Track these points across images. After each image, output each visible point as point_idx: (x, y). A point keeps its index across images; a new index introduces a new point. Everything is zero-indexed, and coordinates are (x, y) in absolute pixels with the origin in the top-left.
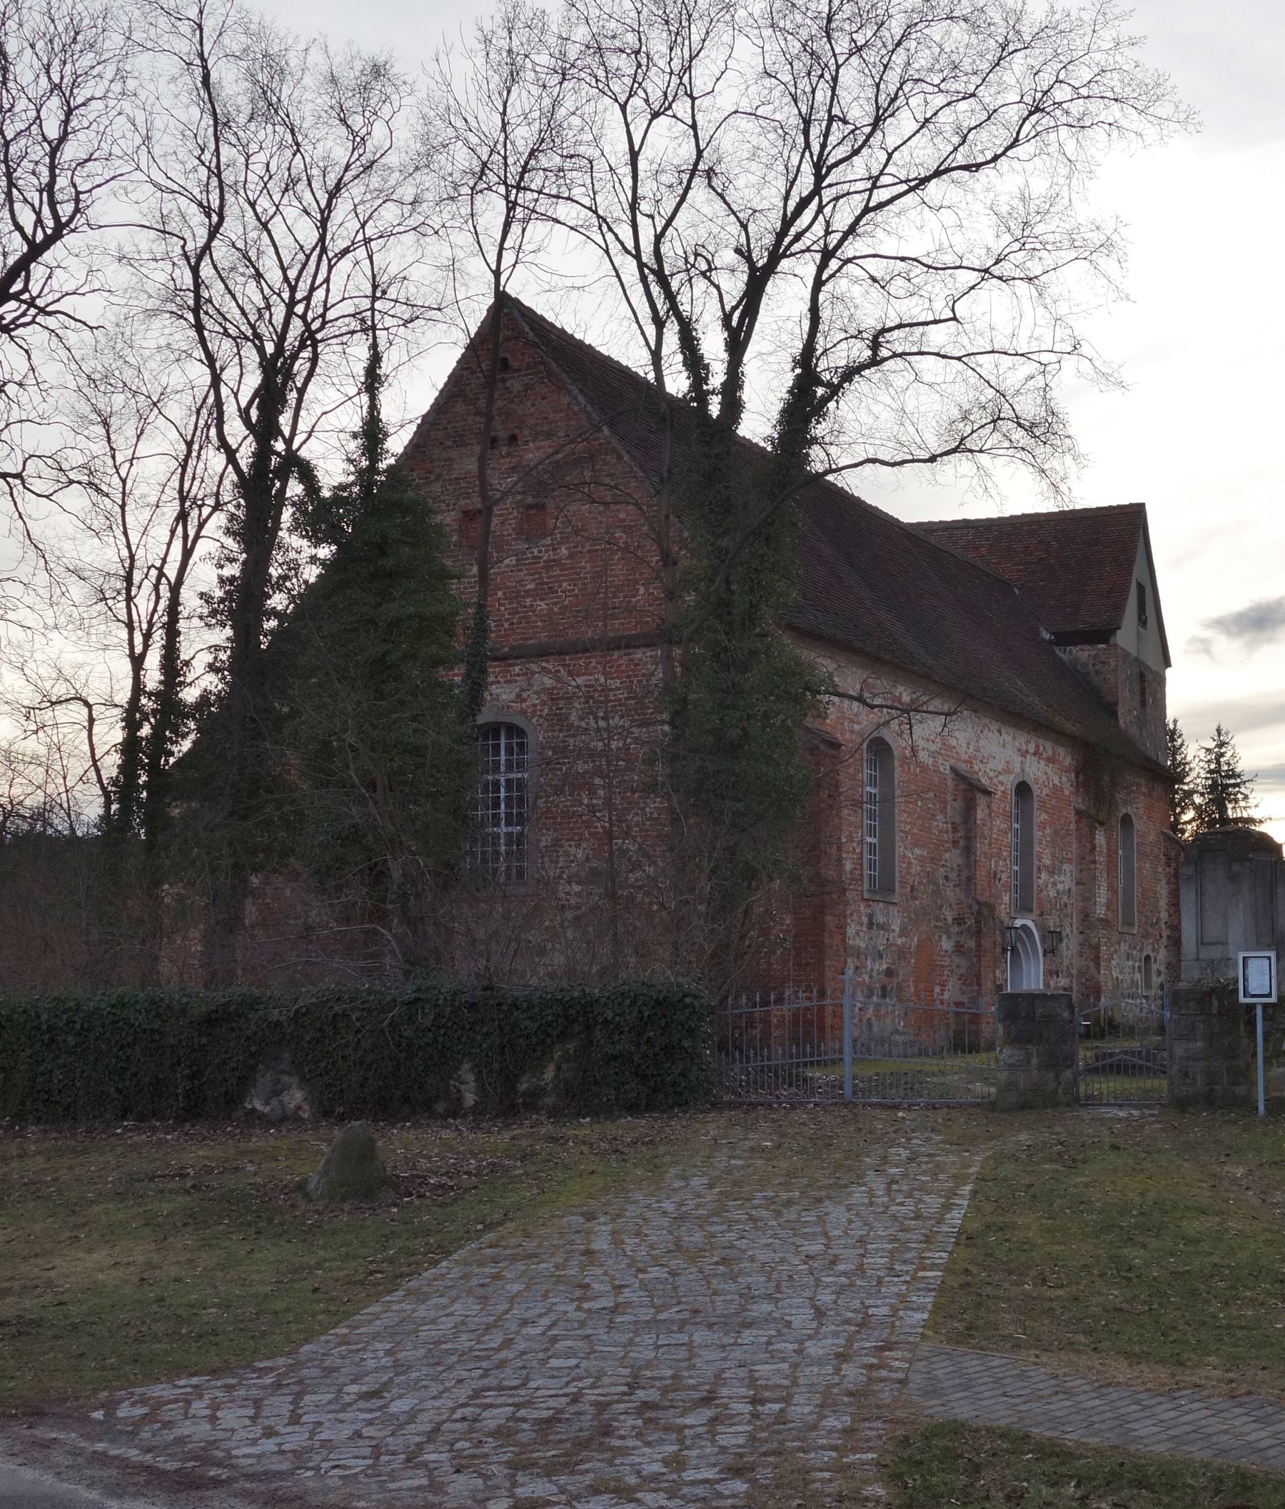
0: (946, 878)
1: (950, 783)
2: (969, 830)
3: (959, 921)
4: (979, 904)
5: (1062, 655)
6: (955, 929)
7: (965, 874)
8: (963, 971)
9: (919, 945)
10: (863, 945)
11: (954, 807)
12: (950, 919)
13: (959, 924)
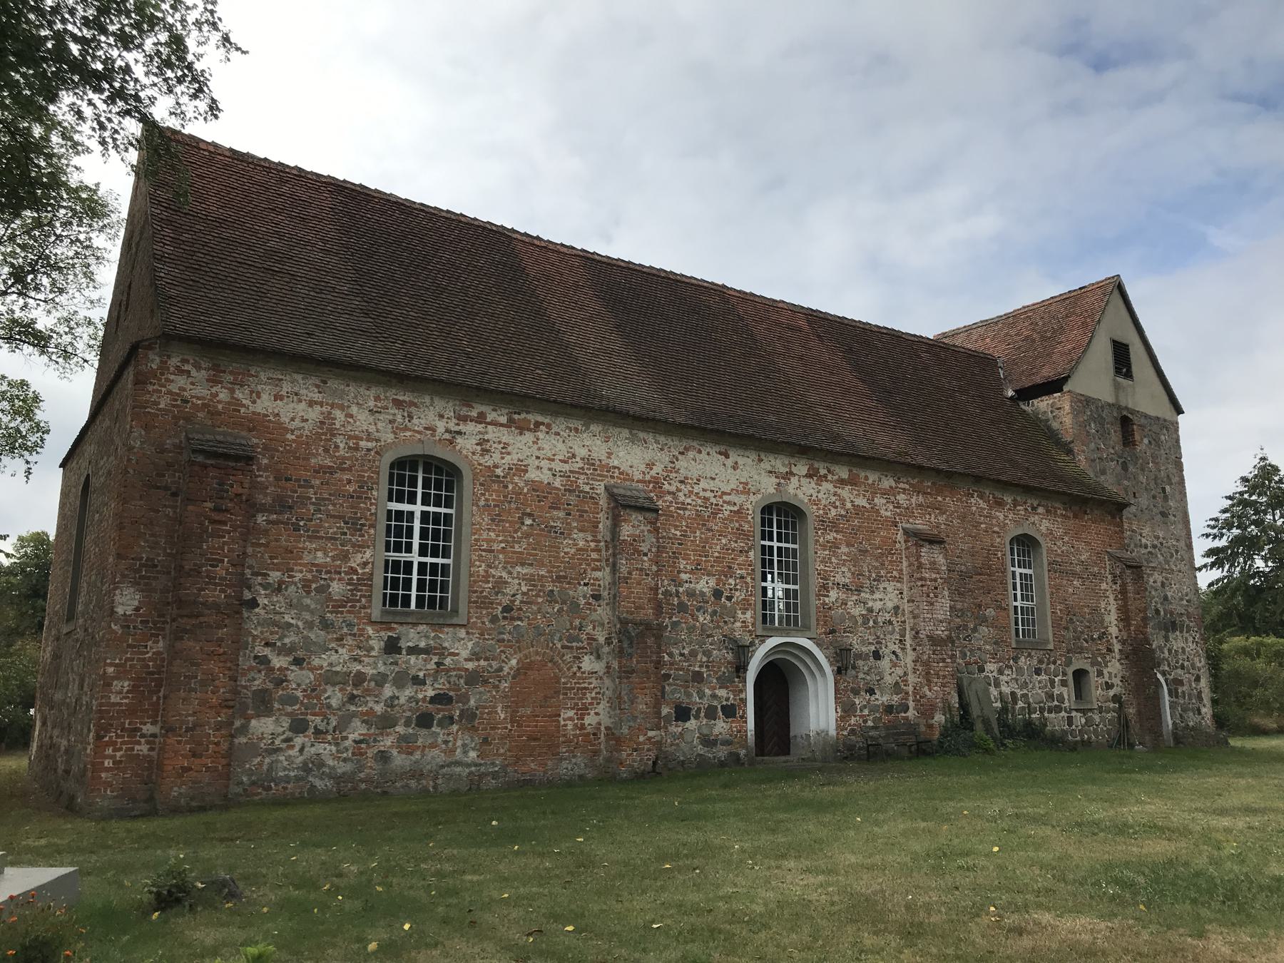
0: (597, 597)
1: (603, 502)
3: (608, 641)
5: (1026, 408)
6: (606, 649)
10: (369, 671)
12: (602, 640)
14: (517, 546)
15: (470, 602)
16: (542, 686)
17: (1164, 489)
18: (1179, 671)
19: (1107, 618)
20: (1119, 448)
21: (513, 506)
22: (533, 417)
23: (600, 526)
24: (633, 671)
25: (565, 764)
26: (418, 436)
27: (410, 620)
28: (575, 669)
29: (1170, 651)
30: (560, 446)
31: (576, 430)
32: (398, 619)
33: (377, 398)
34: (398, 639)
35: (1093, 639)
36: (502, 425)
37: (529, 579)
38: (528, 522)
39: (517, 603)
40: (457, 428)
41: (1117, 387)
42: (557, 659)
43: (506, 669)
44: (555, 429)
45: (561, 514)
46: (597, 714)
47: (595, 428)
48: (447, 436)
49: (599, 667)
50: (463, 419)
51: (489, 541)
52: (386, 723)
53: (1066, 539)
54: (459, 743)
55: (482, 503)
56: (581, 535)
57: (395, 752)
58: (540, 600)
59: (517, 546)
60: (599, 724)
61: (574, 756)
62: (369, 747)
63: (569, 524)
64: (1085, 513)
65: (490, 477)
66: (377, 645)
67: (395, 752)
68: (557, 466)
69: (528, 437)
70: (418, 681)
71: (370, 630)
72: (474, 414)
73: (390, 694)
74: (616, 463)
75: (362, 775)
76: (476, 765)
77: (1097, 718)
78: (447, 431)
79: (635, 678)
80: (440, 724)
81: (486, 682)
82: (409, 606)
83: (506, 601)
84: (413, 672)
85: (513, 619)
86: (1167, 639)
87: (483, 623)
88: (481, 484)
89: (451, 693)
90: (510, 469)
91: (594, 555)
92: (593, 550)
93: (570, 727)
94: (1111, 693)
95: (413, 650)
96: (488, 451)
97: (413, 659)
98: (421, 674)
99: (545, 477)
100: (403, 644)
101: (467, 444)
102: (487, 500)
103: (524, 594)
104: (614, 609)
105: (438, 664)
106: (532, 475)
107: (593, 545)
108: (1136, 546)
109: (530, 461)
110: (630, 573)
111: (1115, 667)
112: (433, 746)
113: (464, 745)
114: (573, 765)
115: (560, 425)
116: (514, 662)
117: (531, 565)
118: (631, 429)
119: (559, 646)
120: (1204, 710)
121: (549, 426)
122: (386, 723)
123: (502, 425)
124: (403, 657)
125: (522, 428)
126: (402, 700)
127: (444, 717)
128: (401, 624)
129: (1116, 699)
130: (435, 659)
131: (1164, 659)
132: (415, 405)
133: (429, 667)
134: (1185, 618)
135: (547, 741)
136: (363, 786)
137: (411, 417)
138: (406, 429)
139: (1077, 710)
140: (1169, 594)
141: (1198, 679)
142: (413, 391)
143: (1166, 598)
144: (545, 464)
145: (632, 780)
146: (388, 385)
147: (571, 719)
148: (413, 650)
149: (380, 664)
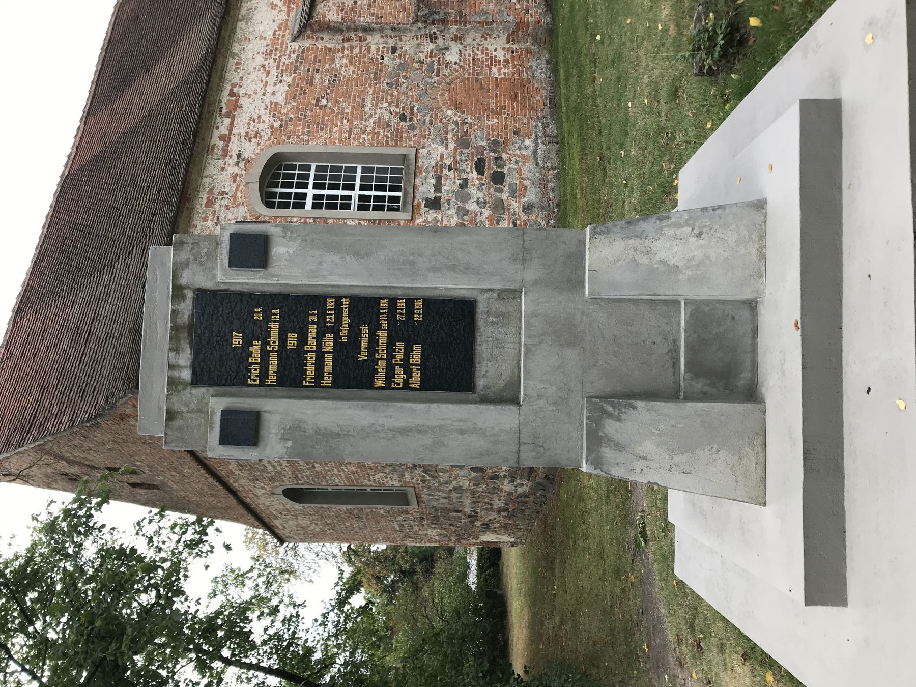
0: (394, 50)
1: (307, 43)
2: (348, 29)
3: (433, 38)
4: (416, 21)
6: (440, 41)
7: (389, 32)
8: (478, 36)
9: (457, 106)
11: (329, 41)
12: (432, 46)
13: (436, 38)
14: (346, 111)
15: (396, 146)
16: (470, 91)
21: (309, 113)
22: (225, 97)
23: (329, 46)
24: (460, 13)
25: (537, 74)
26: (242, 187)
27: (411, 191)
28: (457, 66)
30: (252, 77)
31: (237, 63)
32: (410, 199)
33: (205, 219)
34: (427, 199)
36: (232, 122)
37: (377, 100)
38: (324, 102)
39: (398, 110)
40: (235, 157)
42: (448, 80)
43: (455, 118)
44: (237, 81)
45: (317, 76)
46: (496, 50)
47: (236, 48)
48: (242, 165)
49: (455, 48)
50: (226, 152)
51: (341, 132)
52: (499, 207)
54: (518, 152)
55: (306, 137)
56: (337, 61)
57: (524, 200)
58: (395, 93)
59: (346, 111)
60: (504, 49)
61: (531, 67)
62: (520, 219)
63: (327, 71)
65: (282, 130)
66: (432, 215)
67: (524, 200)
68: (272, 78)
69: (243, 101)
70: (464, 184)
71: (419, 221)
72: (221, 144)
73: (475, 204)
74: (271, 33)
75: (543, 223)
76: (537, 140)
78: (237, 164)
79: (466, 11)
80: (502, 167)
81: (466, 133)
82: (399, 197)
83: (395, 119)
84: (456, 188)
85: (412, 114)
87: (415, 136)
88: (288, 138)
89: (476, 159)
90: (274, 116)
91: (356, 51)
92: (352, 52)
93: (506, 71)
95: (438, 188)
96: (257, 133)
97: (444, 188)
98: (458, 182)
99: (282, 89)
100: (432, 195)
101: (249, 149)
102: (303, 134)
103: (390, 105)
104: (405, 30)
105: (450, 169)
106: (280, 98)
107: (346, 52)
109: (267, 101)
110: (372, 15)
112: (519, 171)
113: (520, 148)
114: (538, 68)
115: (232, 76)
116: (450, 113)
117: (363, 100)
118: (238, 20)
119: (436, 79)
121: (234, 85)
122: (499, 207)
123: (232, 122)
124: (444, 196)
125: (236, 106)
126: (481, 195)
127: (496, 164)
128: (414, 197)
130: (445, 171)
132: (211, 190)
133: (452, 176)
135: (518, 90)
136: (552, 222)
137: (223, 193)
138: (234, 197)
142: (199, 192)
144: (270, 89)
145: (552, 13)
146: (191, 210)
147: (500, 69)
148: (438, 188)
149: (449, 212)
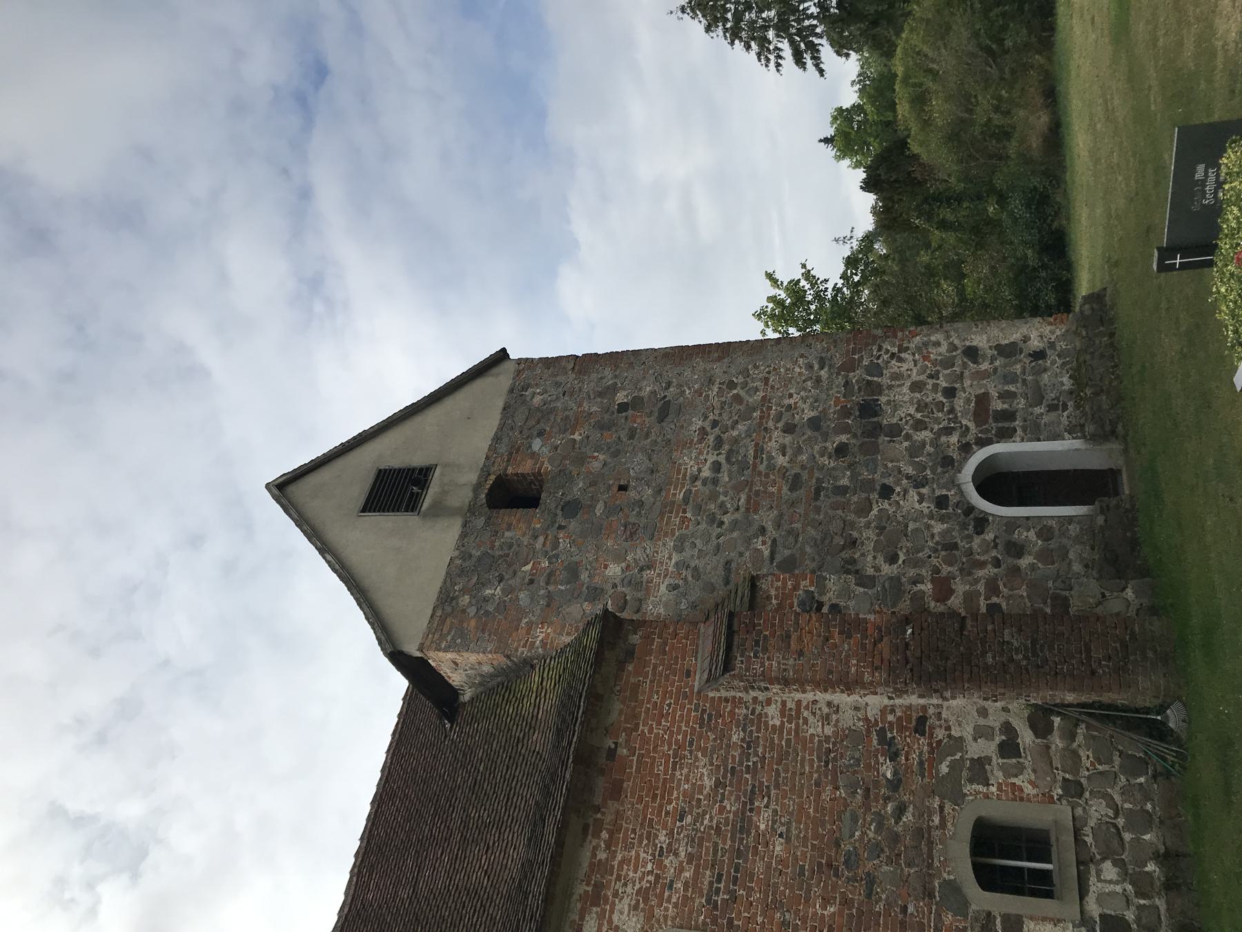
17: (623, 407)
18: (959, 403)
19: (848, 719)
20: (537, 519)
29: (919, 425)
35: (895, 785)
41: (439, 510)
53: (662, 838)
64: (612, 753)
77: (1097, 810)
86: (894, 431)
94: (1026, 737)
108: (713, 496)
111: (963, 713)
120: (1035, 344)
129: (1040, 721)
131: (935, 443)
134: (854, 377)
139: (1083, 893)
140: (809, 414)
141: (972, 353)
143: (815, 424)
